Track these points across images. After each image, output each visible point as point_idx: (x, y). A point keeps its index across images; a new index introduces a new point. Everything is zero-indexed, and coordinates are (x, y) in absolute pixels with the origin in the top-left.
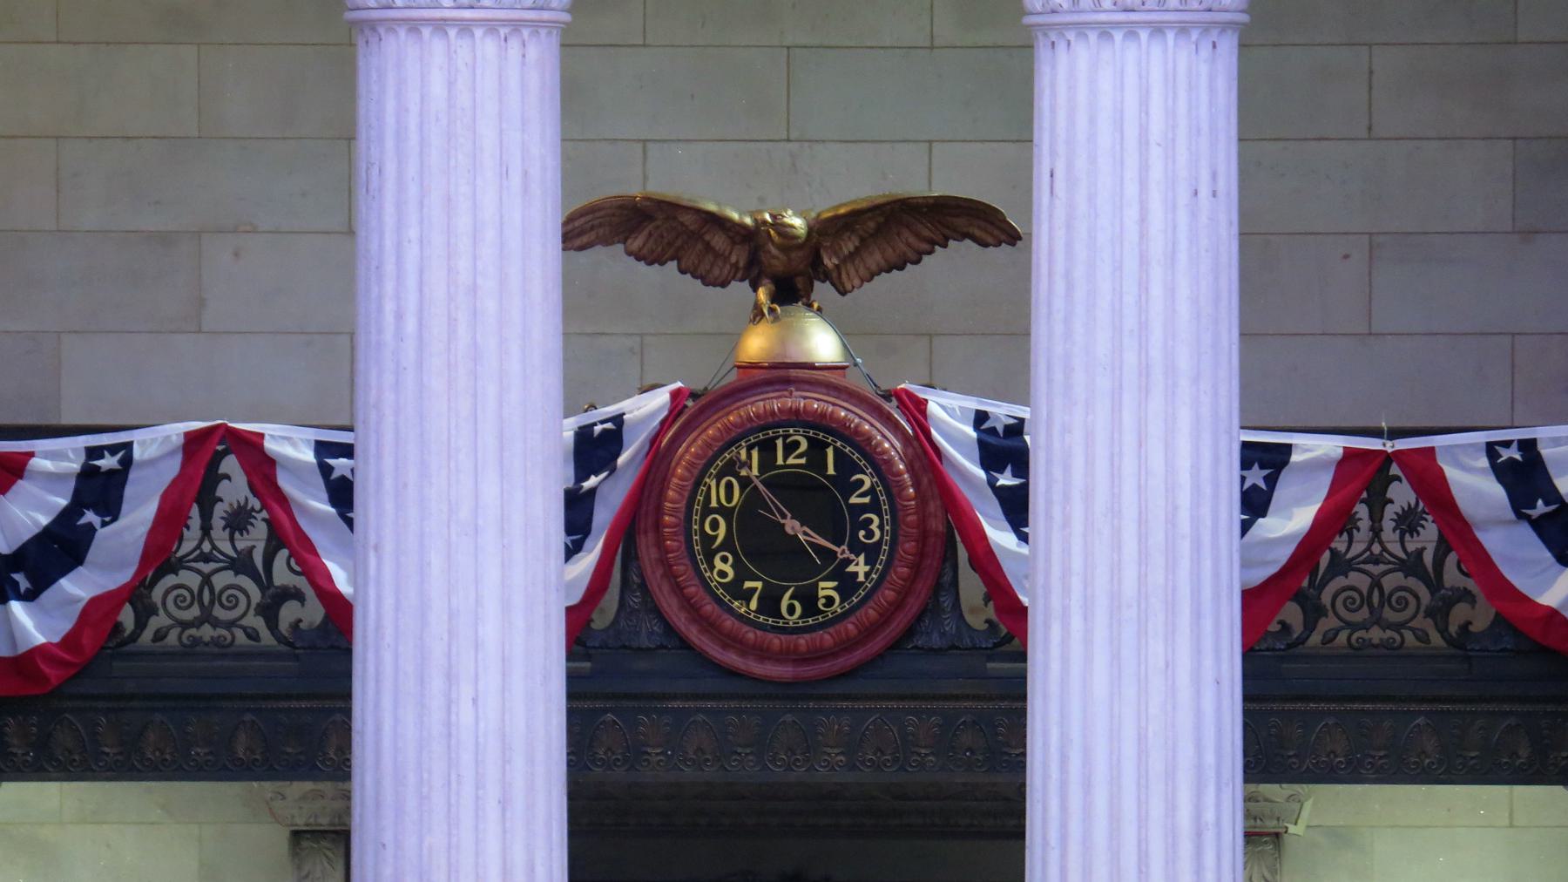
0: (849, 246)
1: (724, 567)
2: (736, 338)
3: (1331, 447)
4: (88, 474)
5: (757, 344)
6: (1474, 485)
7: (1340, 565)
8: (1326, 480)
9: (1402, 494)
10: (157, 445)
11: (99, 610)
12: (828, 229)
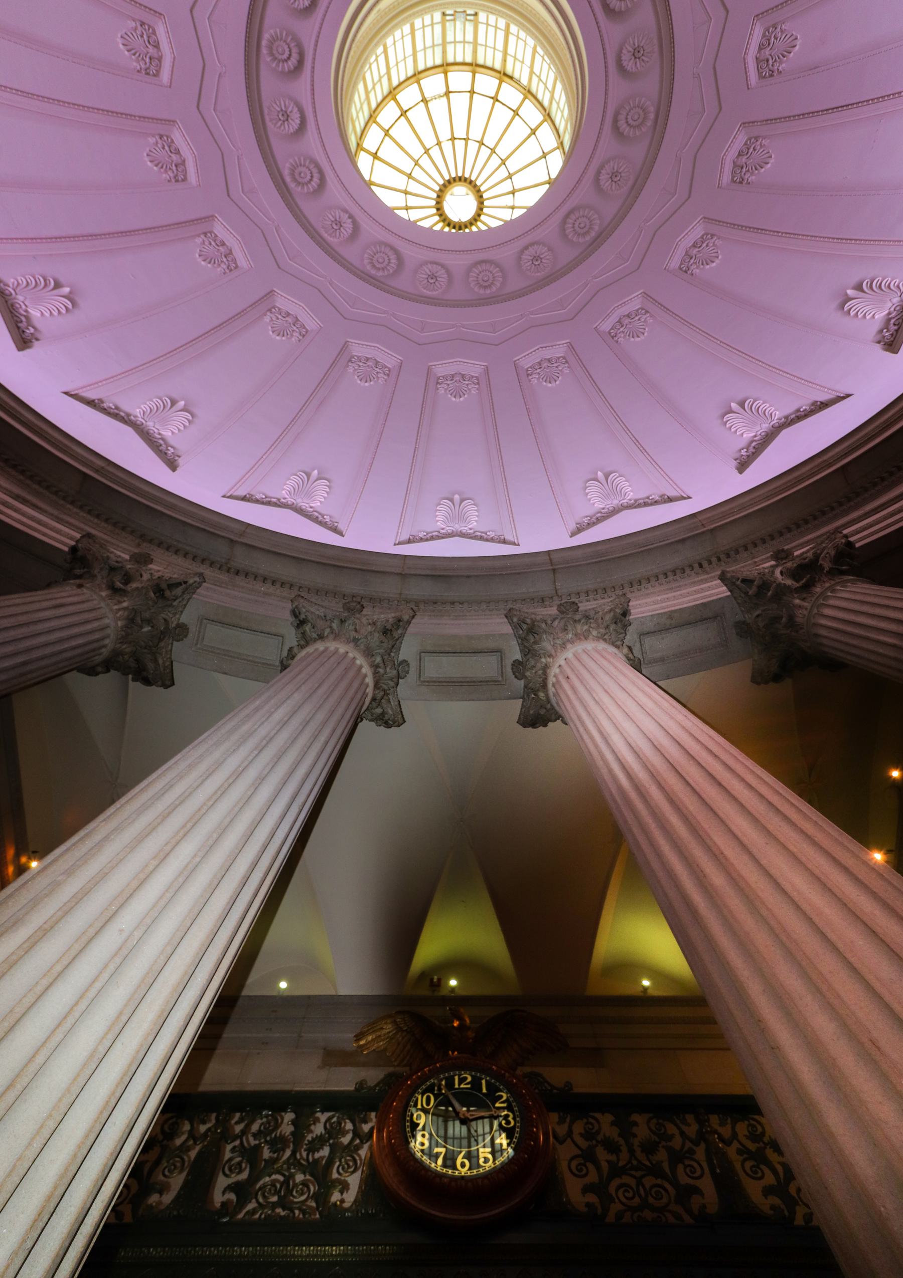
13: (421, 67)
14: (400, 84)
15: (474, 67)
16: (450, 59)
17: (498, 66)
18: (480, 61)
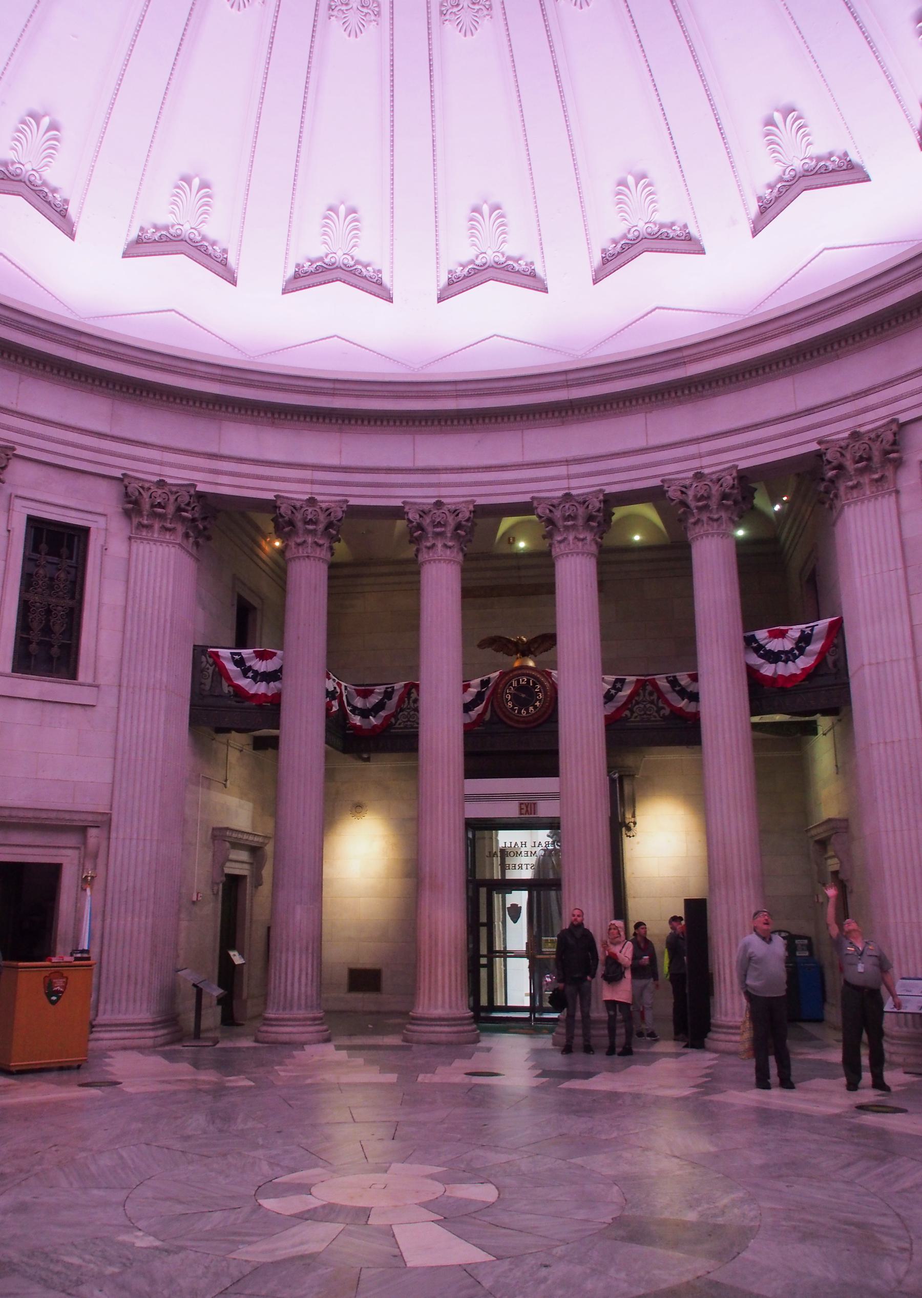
0: (536, 646)
1: (510, 704)
2: (514, 663)
3: (634, 678)
4: (386, 692)
5: (517, 664)
6: (663, 683)
7: (637, 703)
8: (633, 685)
9: (649, 688)
10: (399, 686)
11: (387, 718)
12: (530, 643)
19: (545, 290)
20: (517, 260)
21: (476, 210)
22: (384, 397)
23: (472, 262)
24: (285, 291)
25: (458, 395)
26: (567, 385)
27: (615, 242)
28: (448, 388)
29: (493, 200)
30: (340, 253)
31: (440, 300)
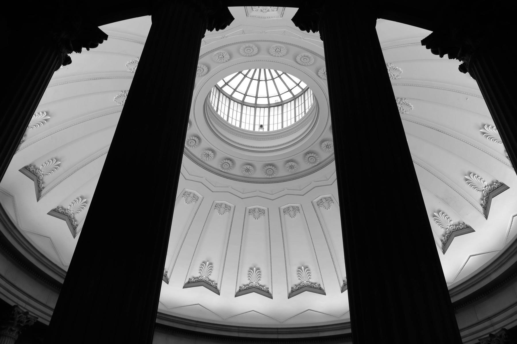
13: (280, 107)
14: (290, 101)
15: (255, 106)
16: (267, 109)
17: (245, 107)
18: (253, 109)
19: (272, 298)
20: (263, 286)
21: (252, 269)
22: (214, 329)
23: (248, 285)
24: (184, 288)
25: (239, 331)
26: (278, 333)
27: (296, 286)
28: (236, 328)
29: (258, 266)
30: (204, 277)
31: (236, 296)
